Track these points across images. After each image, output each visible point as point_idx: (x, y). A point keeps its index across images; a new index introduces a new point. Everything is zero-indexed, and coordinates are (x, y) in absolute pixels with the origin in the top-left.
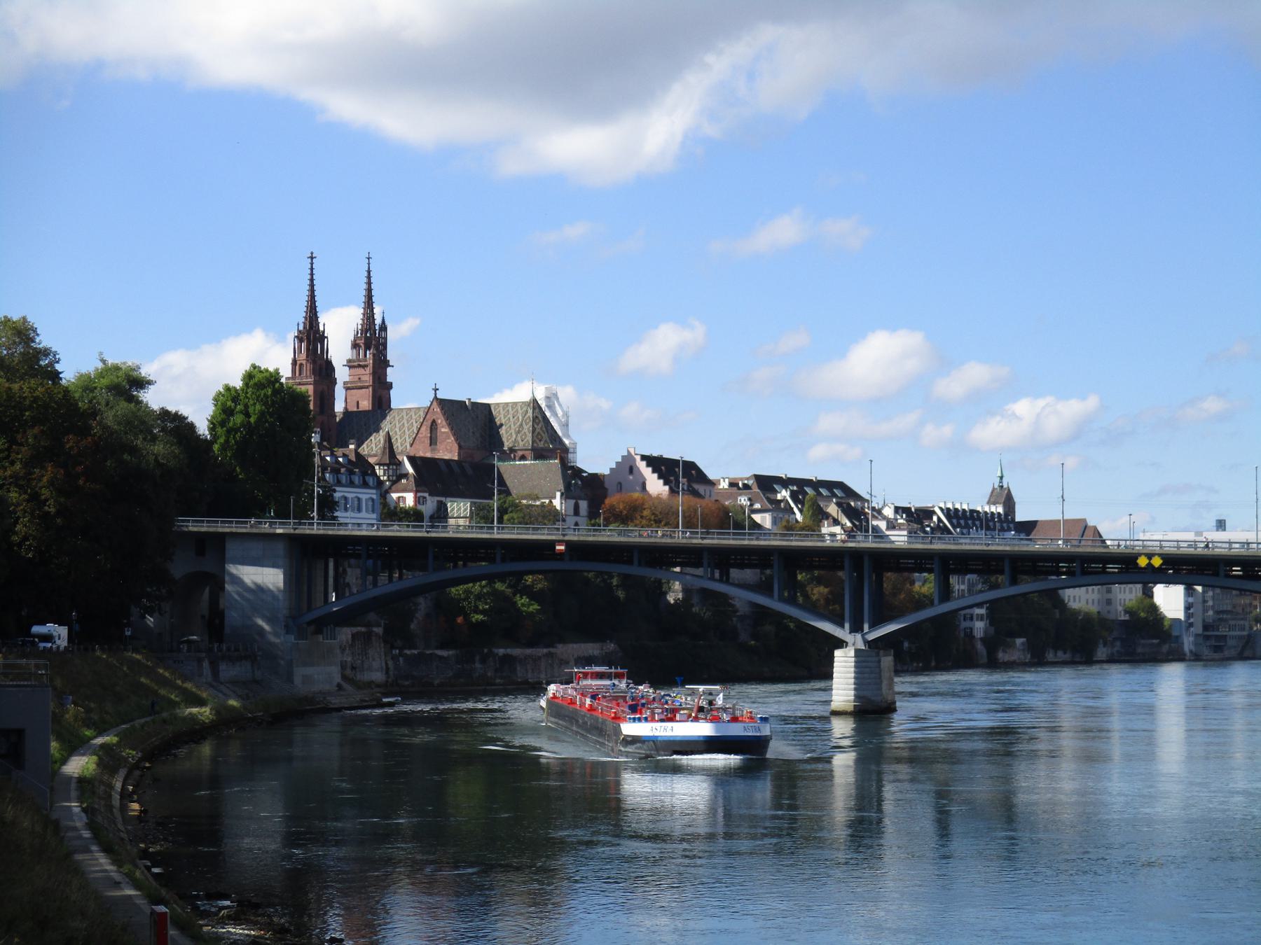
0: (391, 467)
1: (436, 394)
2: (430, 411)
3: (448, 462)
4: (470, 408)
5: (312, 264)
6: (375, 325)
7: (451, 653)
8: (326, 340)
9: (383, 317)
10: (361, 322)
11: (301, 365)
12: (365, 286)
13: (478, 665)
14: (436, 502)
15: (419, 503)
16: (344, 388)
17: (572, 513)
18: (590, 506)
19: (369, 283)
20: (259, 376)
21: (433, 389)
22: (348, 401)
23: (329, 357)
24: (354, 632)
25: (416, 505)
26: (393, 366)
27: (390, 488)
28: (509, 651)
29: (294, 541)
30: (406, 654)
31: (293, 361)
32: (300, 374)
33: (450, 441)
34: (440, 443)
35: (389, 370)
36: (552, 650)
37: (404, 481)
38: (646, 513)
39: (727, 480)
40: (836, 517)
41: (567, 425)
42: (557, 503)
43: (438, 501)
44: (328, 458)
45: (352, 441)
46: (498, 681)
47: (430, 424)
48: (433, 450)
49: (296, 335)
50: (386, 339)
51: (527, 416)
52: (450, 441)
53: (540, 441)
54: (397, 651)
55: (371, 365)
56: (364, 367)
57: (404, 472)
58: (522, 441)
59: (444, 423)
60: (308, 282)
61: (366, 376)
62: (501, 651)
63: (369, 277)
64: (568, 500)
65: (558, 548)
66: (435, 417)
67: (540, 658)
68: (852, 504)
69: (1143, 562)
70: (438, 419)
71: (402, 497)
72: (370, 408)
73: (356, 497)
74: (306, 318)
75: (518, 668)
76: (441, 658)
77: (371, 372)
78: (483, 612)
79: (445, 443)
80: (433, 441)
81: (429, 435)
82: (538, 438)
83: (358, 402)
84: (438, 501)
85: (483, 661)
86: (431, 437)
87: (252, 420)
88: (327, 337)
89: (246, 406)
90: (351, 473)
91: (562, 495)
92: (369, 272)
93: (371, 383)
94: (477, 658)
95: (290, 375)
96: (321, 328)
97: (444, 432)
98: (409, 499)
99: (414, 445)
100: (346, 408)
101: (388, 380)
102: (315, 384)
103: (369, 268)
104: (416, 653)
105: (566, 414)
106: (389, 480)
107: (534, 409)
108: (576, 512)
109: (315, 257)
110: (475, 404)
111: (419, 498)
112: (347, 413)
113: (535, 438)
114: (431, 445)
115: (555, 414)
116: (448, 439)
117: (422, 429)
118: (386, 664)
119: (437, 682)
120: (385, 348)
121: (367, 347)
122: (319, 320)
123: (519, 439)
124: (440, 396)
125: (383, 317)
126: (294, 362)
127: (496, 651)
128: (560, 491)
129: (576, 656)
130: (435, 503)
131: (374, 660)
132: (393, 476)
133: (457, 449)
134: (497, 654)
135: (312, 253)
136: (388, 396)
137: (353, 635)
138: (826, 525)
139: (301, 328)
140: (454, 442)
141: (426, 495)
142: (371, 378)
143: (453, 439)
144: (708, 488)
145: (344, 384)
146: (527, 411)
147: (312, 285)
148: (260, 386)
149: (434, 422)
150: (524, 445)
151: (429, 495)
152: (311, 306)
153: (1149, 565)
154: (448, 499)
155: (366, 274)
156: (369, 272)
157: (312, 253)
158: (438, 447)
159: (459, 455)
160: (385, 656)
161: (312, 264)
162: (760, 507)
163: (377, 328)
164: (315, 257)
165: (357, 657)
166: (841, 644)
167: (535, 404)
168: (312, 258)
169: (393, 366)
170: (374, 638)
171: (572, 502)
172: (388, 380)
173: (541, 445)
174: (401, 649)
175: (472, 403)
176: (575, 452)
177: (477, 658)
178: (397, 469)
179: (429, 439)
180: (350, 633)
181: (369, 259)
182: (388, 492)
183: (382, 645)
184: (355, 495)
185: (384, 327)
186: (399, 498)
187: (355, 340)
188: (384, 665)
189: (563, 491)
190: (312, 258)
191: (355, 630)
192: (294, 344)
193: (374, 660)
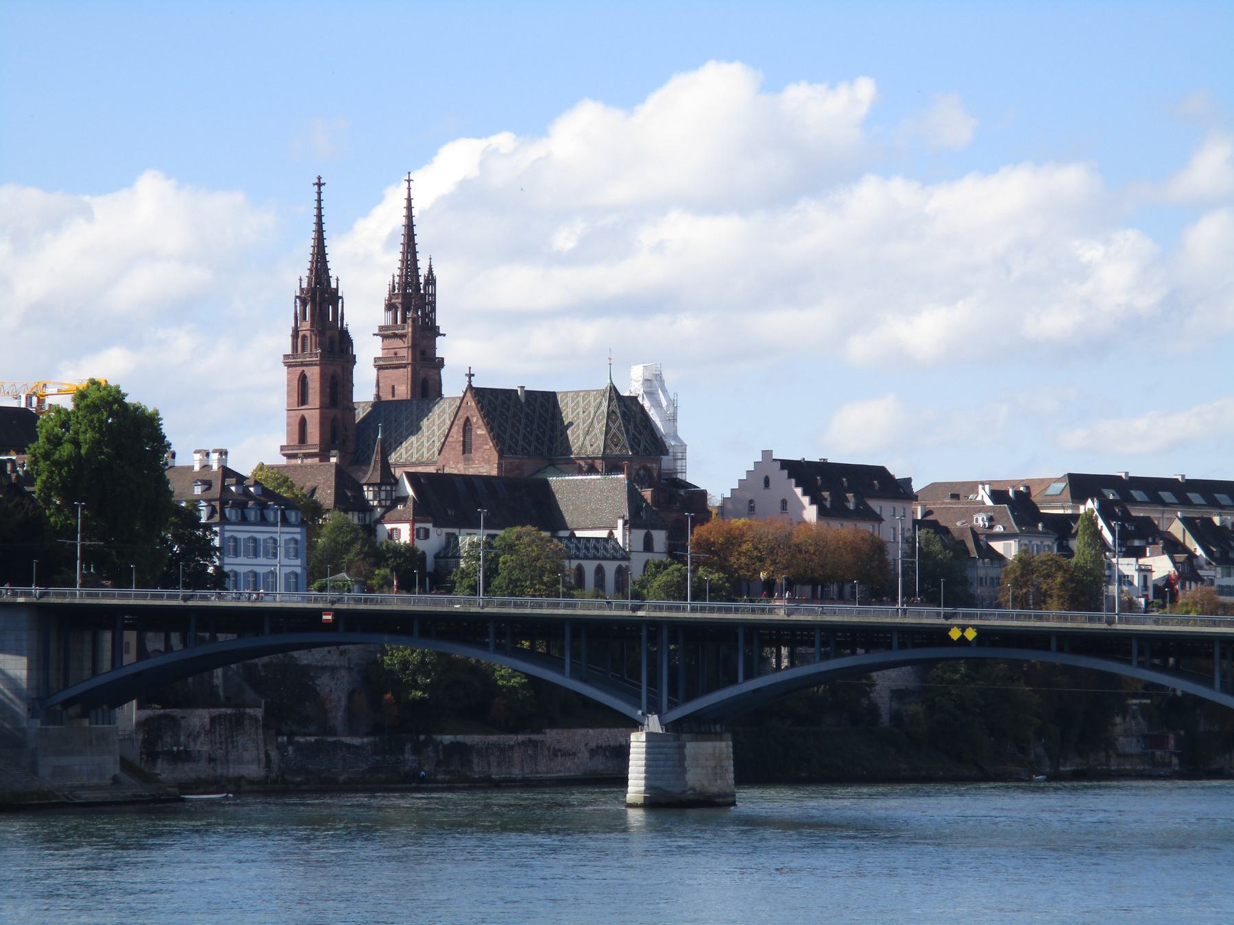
0: (383, 488)
2: (463, 405)
3: (487, 479)
4: (523, 400)
5: (319, 193)
6: (418, 276)
7: (366, 740)
8: (340, 300)
9: (430, 266)
10: (398, 272)
11: (304, 337)
13: (408, 756)
14: (444, 535)
15: (418, 537)
16: (375, 366)
17: (641, 548)
18: (669, 537)
20: (94, 395)
21: (466, 375)
22: (381, 385)
23: (345, 323)
24: (214, 715)
25: (413, 540)
26: (444, 335)
27: (382, 516)
28: (460, 738)
29: (41, 611)
30: (298, 742)
31: (293, 331)
32: (303, 350)
33: (488, 447)
34: (475, 450)
35: (438, 339)
36: (534, 737)
37: (400, 507)
38: (744, 547)
39: (987, 487)
40: (1182, 540)
41: (675, 420)
42: (618, 534)
43: (447, 534)
44: (233, 488)
45: (334, 452)
46: (440, 777)
47: (462, 423)
48: (467, 461)
49: (298, 294)
50: (434, 295)
51: (599, 412)
52: (488, 447)
53: (616, 445)
54: (285, 738)
55: (410, 334)
56: (402, 336)
57: (403, 495)
58: (592, 445)
59: (480, 422)
61: (403, 350)
62: (447, 739)
64: (633, 531)
65: (325, 617)
66: (468, 414)
67: (511, 748)
68: (1217, 520)
69: (955, 634)
70: (473, 416)
71: (396, 529)
72: (409, 398)
73: (271, 538)
74: (311, 270)
75: (475, 761)
76: (349, 747)
77: (410, 345)
78: (424, 688)
79: (482, 450)
80: (466, 447)
81: (462, 439)
82: (612, 442)
83: (393, 387)
84: (447, 534)
85: (417, 750)
86: (464, 442)
87: (83, 451)
88: (341, 298)
89: (77, 433)
90: (262, 507)
91: (625, 523)
92: (409, 200)
93: (410, 361)
94: (408, 746)
95: (289, 351)
96: (333, 285)
97: (481, 436)
98: (405, 534)
99: (442, 453)
100: (378, 396)
101: (438, 355)
102: (322, 364)
104: (313, 740)
105: (673, 404)
106: (380, 506)
107: (610, 400)
108: (648, 546)
109: (324, 184)
110: (530, 394)
111: (418, 530)
112: (379, 405)
113: (609, 442)
114: (464, 453)
115: (657, 404)
116: (486, 444)
117: (452, 430)
118: (267, 756)
119: (342, 778)
120: (434, 310)
121: (406, 309)
122: (331, 273)
123: (587, 443)
125: (430, 266)
126: (296, 332)
127: (438, 738)
128: (623, 517)
129: (593, 745)
130: (443, 537)
131: (245, 749)
132: (386, 500)
133: (497, 458)
134: (441, 742)
135: (319, 178)
136: (437, 377)
137: (213, 720)
138: (1148, 554)
139: (305, 285)
140: (493, 449)
141: (429, 526)
142: (410, 352)
143: (491, 444)
144: (899, 505)
145: (375, 362)
146: (600, 403)
147: (320, 224)
148: (94, 408)
149: (467, 420)
150: (593, 452)
151: (434, 526)
152: (318, 254)
153: (963, 639)
154: (464, 531)
155: (405, 203)
156: (409, 200)
157: (319, 178)
158: (472, 455)
159: (500, 466)
160: (265, 744)
161: (319, 193)
162: (1002, 530)
163: (422, 280)
164: (324, 184)
165: (218, 745)
166: (636, 725)
167: (613, 394)
168: (319, 185)
169: (444, 335)
170: (247, 722)
171: (640, 534)
172: (438, 355)
173: (616, 451)
174: (291, 735)
175: (526, 391)
176: (684, 459)
177: (408, 746)
178: (392, 491)
179: (461, 444)
180: (207, 716)
182: (380, 521)
183: (260, 731)
184: (269, 535)
185: (431, 280)
186: (392, 530)
187: (390, 298)
188: (262, 756)
189: (627, 518)
190: (319, 185)
191: (215, 712)
192: (296, 307)
193: (245, 749)
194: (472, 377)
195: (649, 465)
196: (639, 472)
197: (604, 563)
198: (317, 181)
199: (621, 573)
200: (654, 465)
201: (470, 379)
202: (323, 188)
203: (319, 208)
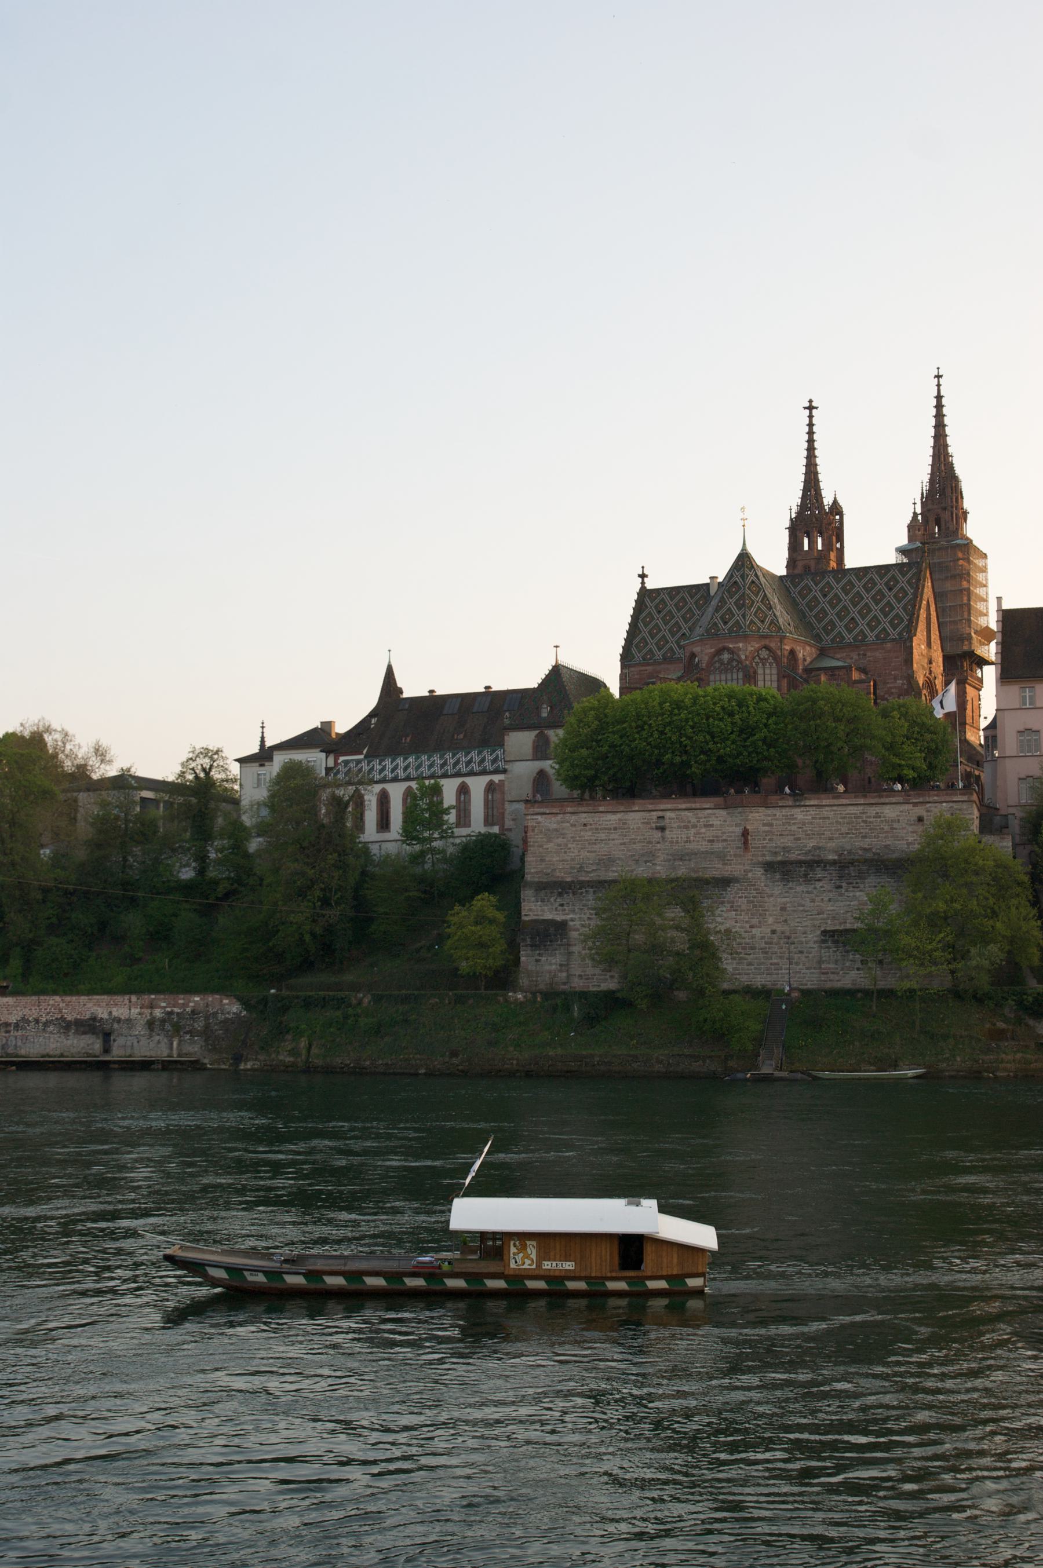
1: (643, 583)
5: (811, 417)
12: (933, 422)
19: (939, 416)
21: (640, 576)
60: (806, 445)
63: (939, 407)
92: (939, 397)
103: (939, 391)
108: (540, 750)
124: (650, 585)
135: (810, 401)
155: (934, 402)
156: (939, 397)
157: (810, 401)
161: (811, 417)
168: (811, 408)
181: (938, 377)
190: (811, 408)
194: (645, 579)
195: (731, 646)
196: (722, 657)
197: (469, 780)
198: (807, 405)
199: (490, 788)
200: (741, 645)
203: (811, 433)
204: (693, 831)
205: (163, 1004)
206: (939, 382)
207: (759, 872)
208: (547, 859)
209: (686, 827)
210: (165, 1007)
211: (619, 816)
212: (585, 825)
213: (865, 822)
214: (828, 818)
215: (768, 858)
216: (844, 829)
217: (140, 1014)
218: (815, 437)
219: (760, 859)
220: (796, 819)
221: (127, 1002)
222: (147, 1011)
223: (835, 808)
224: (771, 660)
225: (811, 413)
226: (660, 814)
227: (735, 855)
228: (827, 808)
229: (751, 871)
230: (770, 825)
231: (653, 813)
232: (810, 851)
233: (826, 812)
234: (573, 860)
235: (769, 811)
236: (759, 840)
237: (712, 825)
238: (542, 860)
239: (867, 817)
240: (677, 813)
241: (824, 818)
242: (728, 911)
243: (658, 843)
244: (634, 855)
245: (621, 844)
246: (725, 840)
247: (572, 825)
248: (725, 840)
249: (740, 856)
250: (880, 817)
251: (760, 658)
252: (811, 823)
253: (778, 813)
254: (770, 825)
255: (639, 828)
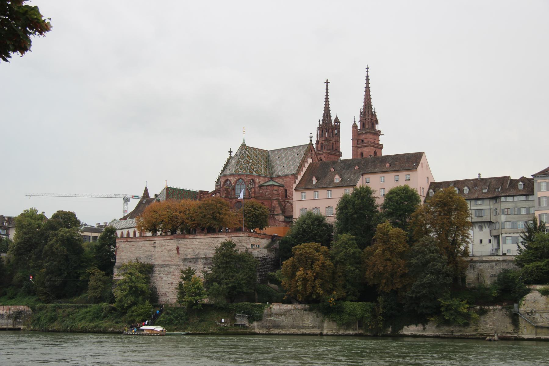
1: (230, 155)
5: (327, 86)
12: (365, 86)
19: (367, 83)
21: (229, 152)
60: (325, 97)
63: (367, 80)
92: (368, 76)
103: (367, 74)
109: (329, 82)
135: (327, 80)
147: (327, 98)
156: (368, 76)
157: (327, 80)
161: (327, 86)
164: (329, 82)
168: (327, 83)
181: (367, 68)
190: (327, 83)
200: (232, 178)
201: (230, 153)
202: (329, 84)
203: (327, 92)
204: (164, 247)
205: (13, 309)
206: (367, 70)
207: (181, 262)
208: (122, 258)
209: (162, 246)
210: (13, 310)
211: (143, 242)
212: (133, 246)
213: (214, 244)
214: (203, 242)
215: (185, 257)
216: (207, 247)
217: (6, 312)
218: (329, 94)
219: (183, 257)
220: (193, 243)
221: (2, 308)
222: (8, 311)
223: (205, 239)
224: (243, 183)
225: (327, 84)
226: (155, 241)
227: (175, 256)
228: (203, 239)
229: (179, 261)
230: (186, 245)
231: (153, 241)
232: (197, 254)
233: (202, 240)
234: (129, 258)
235: (186, 240)
236: (182, 250)
237: (169, 245)
238: (120, 258)
239: (214, 242)
240: (160, 241)
241: (202, 243)
242: (172, 276)
243: (153, 252)
244: (146, 256)
245: (143, 252)
246: (173, 251)
247: (130, 246)
248: (173, 251)
249: (177, 256)
250: (218, 242)
251: (239, 183)
252: (198, 244)
253: (189, 241)
254: (186, 245)
255: (148, 246)
